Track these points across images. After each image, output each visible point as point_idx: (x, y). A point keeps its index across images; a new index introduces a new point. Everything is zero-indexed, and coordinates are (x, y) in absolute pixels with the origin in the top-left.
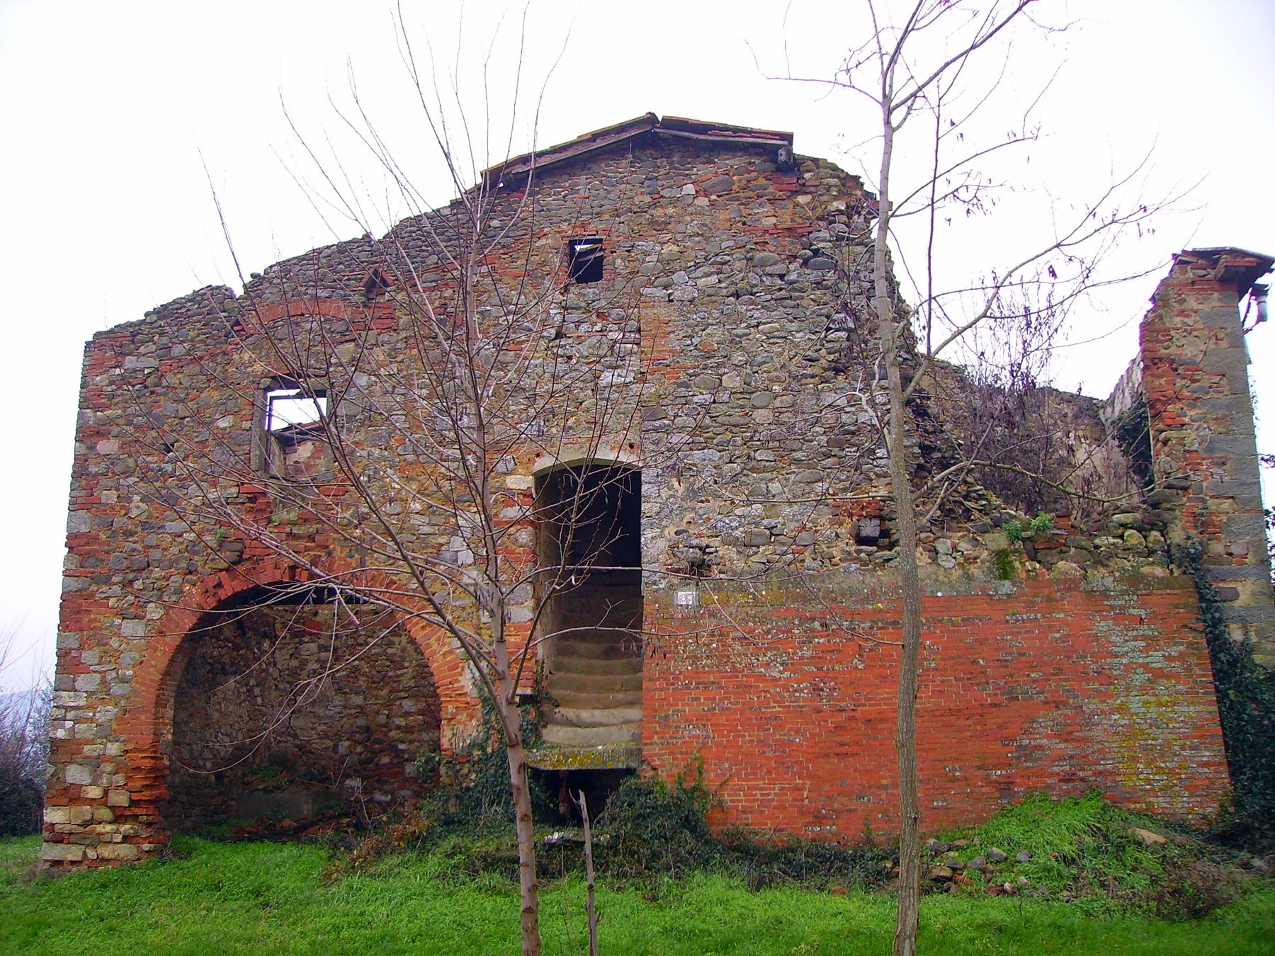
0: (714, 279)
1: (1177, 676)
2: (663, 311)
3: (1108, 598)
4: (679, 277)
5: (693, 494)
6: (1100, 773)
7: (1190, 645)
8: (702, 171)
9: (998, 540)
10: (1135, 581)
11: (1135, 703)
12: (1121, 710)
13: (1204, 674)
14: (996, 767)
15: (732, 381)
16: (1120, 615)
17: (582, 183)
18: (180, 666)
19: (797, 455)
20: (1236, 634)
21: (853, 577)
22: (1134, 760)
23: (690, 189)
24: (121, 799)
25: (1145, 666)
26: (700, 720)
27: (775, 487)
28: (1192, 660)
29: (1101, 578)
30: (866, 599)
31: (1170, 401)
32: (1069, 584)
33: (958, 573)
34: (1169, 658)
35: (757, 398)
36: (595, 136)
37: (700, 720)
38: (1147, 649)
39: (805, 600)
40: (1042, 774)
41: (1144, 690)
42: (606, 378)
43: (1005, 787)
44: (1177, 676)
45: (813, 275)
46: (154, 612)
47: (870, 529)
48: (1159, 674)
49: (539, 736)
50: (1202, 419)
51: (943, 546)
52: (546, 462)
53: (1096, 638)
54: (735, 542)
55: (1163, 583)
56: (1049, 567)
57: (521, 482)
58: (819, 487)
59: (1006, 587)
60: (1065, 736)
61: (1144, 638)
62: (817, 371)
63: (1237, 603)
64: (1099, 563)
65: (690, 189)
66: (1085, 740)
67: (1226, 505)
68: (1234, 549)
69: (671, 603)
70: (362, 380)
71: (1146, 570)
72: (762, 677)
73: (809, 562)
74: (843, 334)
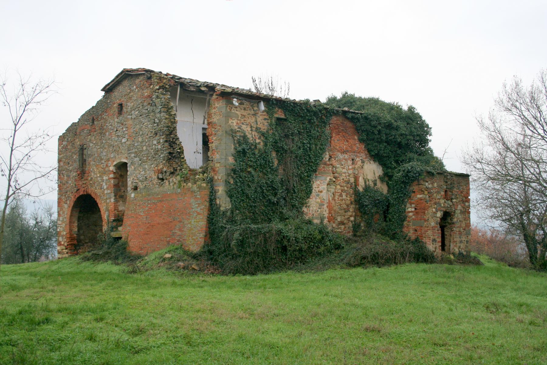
0: (137, 112)
1: (201, 214)
2: (130, 122)
3: (195, 193)
4: (133, 112)
5: (135, 168)
6: (184, 240)
7: (205, 206)
8: (137, 81)
9: (179, 178)
10: (200, 187)
11: (193, 223)
12: (190, 223)
13: (206, 213)
14: (169, 237)
15: (140, 140)
16: (196, 198)
17: (120, 88)
18: (76, 214)
19: (149, 158)
20: (218, 202)
21: (157, 189)
22: (189, 236)
23: (135, 87)
24: (66, 244)
25: (196, 211)
26: (129, 225)
27: (146, 166)
28: (205, 210)
29: (195, 187)
30: (158, 195)
31: (211, 135)
32: (189, 189)
33: (172, 187)
34: (201, 209)
35: (144, 144)
36: (117, 77)
37: (129, 225)
38: (198, 206)
39: (149, 195)
40: (175, 239)
41: (195, 218)
42: (123, 141)
43: (168, 242)
44: (201, 214)
45: (152, 108)
46: (68, 202)
47: (161, 176)
48: (199, 214)
49: (117, 229)
50: (216, 140)
51: (171, 180)
52: (115, 163)
53: (190, 204)
54: (141, 181)
55: (205, 188)
56: (187, 184)
57: (112, 168)
58: (152, 166)
59: (179, 190)
60: (180, 230)
61: (198, 204)
62: (152, 135)
63: (219, 193)
64: (195, 183)
65: (135, 87)
66: (183, 231)
67: (218, 165)
68: (220, 178)
69: (130, 197)
70: (91, 145)
71: (202, 185)
72: (140, 215)
73: (151, 186)
74: (156, 124)
